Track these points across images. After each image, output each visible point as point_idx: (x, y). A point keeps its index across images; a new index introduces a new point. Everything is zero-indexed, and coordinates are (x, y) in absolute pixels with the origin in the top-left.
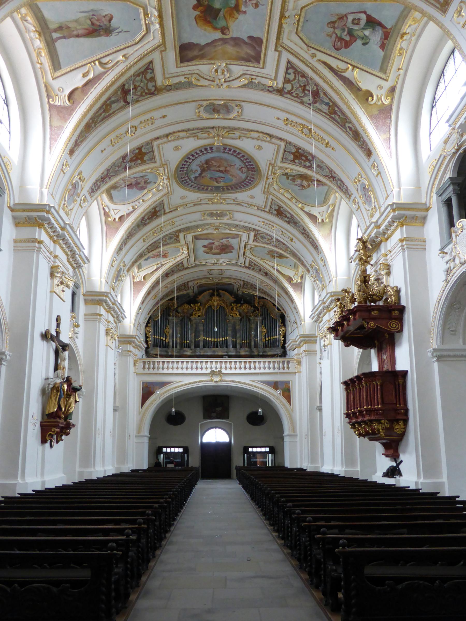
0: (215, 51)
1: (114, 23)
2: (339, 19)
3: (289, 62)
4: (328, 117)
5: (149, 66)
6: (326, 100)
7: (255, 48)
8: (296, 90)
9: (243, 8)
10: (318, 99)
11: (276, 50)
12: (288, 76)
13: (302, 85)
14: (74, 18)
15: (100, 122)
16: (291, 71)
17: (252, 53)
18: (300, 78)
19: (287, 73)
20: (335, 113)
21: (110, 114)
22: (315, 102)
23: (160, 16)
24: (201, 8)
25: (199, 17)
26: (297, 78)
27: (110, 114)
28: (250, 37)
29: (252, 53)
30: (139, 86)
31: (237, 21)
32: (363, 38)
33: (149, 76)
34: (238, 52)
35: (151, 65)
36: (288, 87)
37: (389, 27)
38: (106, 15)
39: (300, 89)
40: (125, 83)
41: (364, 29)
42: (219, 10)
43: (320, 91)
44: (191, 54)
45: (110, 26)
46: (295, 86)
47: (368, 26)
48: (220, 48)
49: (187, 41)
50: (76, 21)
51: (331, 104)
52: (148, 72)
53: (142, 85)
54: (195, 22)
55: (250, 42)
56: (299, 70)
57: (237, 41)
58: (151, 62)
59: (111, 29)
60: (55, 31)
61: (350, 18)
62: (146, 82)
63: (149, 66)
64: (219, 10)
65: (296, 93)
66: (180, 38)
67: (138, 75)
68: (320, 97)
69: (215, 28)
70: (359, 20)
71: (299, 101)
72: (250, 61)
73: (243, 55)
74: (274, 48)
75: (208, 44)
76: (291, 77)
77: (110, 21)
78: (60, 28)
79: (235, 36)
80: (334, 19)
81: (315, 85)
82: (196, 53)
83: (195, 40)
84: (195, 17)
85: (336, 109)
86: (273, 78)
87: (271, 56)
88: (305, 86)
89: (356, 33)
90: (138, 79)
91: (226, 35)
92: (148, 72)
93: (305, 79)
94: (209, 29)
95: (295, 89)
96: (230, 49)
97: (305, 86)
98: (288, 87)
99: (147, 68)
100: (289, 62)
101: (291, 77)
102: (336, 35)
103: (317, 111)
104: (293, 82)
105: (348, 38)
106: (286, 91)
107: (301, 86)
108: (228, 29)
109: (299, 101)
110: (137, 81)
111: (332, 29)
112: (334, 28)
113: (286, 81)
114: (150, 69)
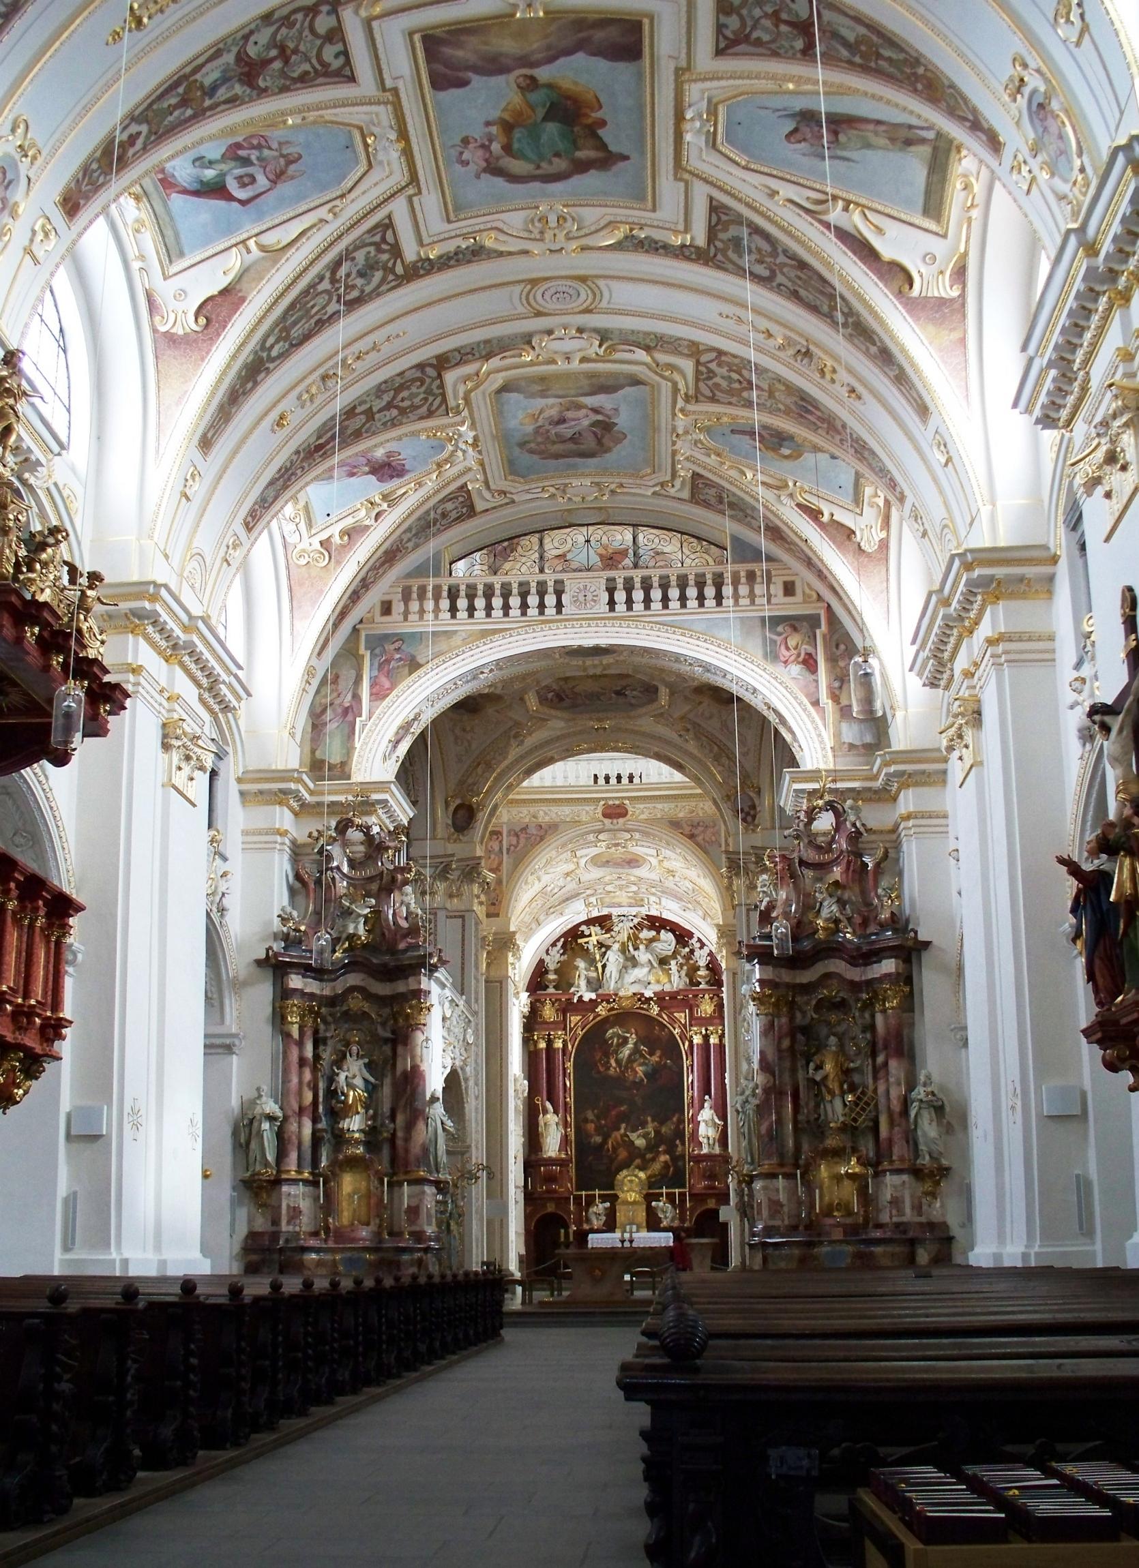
0: (547, 36)
1: (790, 126)
2: (282, 173)
3: (352, 79)
4: (188, 70)
5: (727, 47)
6: (222, 94)
7: (446, 66)
8: (301, 33)
9: (494, 130)
10: (240, 70)
11: (395, 91)
12: (340, 47)
13: (294, 57)
14: (869, 153)
15: (902, 50)
16: (337, 64)
17: (448, 51)
18: (307, 67)
19: (345, 53)
20: (184, 102)
21: (868, 26)
22: (241, 58)
23: (679, 117)
24: (590, 121)
25: (592, 109)
26: (314, 61)
27: (868, 26)
28: (463, 83)
29: (448, 51)
30: (766, 15)
31: (503, 105)
32: (211, 162)
33: (733, 22)
34: (486, 43)
35: (722, 45)
36: (323, 23)
37: (174, 195)
38: (800, 142)
39: (291, 45)
40: (799, 55)
41: (222, 175)
42: (545, 119)
43: (248, 91)
44: (612, 34)
45: (798, 123)
46: (310, 37)
47: (217, 183)
48: (535, 46)
49: (621, 66)
50: (868, 146)
51: (207, 103)
52: (734, 32)
53: (757, 12)
54: (602, 100)
55: (460, 74)
56: (321, 80)
57: (494, 66)
58: (719, 52)
59: (798, 118)
60: (923, 141)
61: (262, 181)
62: (744, 12)
63: (727, 47)
64: (545, 119)
65: (298, 26)
66: (640, 75)
67: (758, 42)
68: (240, 80)
69: (550, 86)
70: (243, 185)
71: (276, 16)
72: (448, 32)
73: (473, 41)
74: (403, 95)
75: (568, 52)
76: (329, 52)
77: (796, 130)
78: (909, 142)
79: (500, 80)
80: (292, 167)
81: (265, 90)
82: (599, 35)
83: (602, 64)
84: (601, 107)
85: (189, 112)
86: (375, 24)
87: (401, 62)
88: (286, 61)
89: (233, 164)
90: (766, 38)
91: (526, 76)
92: (734, 32)
93: (295, 75)
94: (566, 84)
95: (306, 32)
96: (508, 45)
97: (286, 61)
98: (323, 23)
99: (734, 43)
100: (352, 79)
101: (329, 52)
102: (270, 148)
103: (221, 46)
104: (318, 42)
105: (241, 153)
106: (325, 8)
107: (295, 51)
108: (519, 87)
109: (276, 16)
110: (766, 30)
111: (285, 152)
112: (282, 156)
113: (336, 34)
114: (726, 38)
